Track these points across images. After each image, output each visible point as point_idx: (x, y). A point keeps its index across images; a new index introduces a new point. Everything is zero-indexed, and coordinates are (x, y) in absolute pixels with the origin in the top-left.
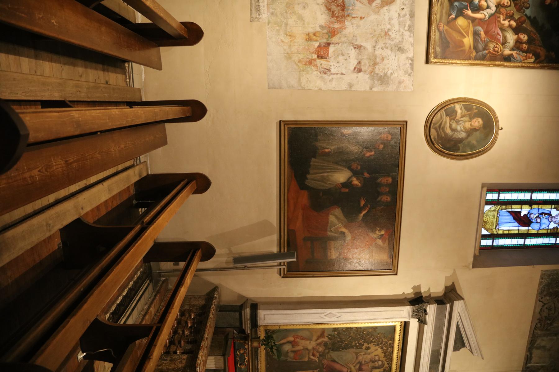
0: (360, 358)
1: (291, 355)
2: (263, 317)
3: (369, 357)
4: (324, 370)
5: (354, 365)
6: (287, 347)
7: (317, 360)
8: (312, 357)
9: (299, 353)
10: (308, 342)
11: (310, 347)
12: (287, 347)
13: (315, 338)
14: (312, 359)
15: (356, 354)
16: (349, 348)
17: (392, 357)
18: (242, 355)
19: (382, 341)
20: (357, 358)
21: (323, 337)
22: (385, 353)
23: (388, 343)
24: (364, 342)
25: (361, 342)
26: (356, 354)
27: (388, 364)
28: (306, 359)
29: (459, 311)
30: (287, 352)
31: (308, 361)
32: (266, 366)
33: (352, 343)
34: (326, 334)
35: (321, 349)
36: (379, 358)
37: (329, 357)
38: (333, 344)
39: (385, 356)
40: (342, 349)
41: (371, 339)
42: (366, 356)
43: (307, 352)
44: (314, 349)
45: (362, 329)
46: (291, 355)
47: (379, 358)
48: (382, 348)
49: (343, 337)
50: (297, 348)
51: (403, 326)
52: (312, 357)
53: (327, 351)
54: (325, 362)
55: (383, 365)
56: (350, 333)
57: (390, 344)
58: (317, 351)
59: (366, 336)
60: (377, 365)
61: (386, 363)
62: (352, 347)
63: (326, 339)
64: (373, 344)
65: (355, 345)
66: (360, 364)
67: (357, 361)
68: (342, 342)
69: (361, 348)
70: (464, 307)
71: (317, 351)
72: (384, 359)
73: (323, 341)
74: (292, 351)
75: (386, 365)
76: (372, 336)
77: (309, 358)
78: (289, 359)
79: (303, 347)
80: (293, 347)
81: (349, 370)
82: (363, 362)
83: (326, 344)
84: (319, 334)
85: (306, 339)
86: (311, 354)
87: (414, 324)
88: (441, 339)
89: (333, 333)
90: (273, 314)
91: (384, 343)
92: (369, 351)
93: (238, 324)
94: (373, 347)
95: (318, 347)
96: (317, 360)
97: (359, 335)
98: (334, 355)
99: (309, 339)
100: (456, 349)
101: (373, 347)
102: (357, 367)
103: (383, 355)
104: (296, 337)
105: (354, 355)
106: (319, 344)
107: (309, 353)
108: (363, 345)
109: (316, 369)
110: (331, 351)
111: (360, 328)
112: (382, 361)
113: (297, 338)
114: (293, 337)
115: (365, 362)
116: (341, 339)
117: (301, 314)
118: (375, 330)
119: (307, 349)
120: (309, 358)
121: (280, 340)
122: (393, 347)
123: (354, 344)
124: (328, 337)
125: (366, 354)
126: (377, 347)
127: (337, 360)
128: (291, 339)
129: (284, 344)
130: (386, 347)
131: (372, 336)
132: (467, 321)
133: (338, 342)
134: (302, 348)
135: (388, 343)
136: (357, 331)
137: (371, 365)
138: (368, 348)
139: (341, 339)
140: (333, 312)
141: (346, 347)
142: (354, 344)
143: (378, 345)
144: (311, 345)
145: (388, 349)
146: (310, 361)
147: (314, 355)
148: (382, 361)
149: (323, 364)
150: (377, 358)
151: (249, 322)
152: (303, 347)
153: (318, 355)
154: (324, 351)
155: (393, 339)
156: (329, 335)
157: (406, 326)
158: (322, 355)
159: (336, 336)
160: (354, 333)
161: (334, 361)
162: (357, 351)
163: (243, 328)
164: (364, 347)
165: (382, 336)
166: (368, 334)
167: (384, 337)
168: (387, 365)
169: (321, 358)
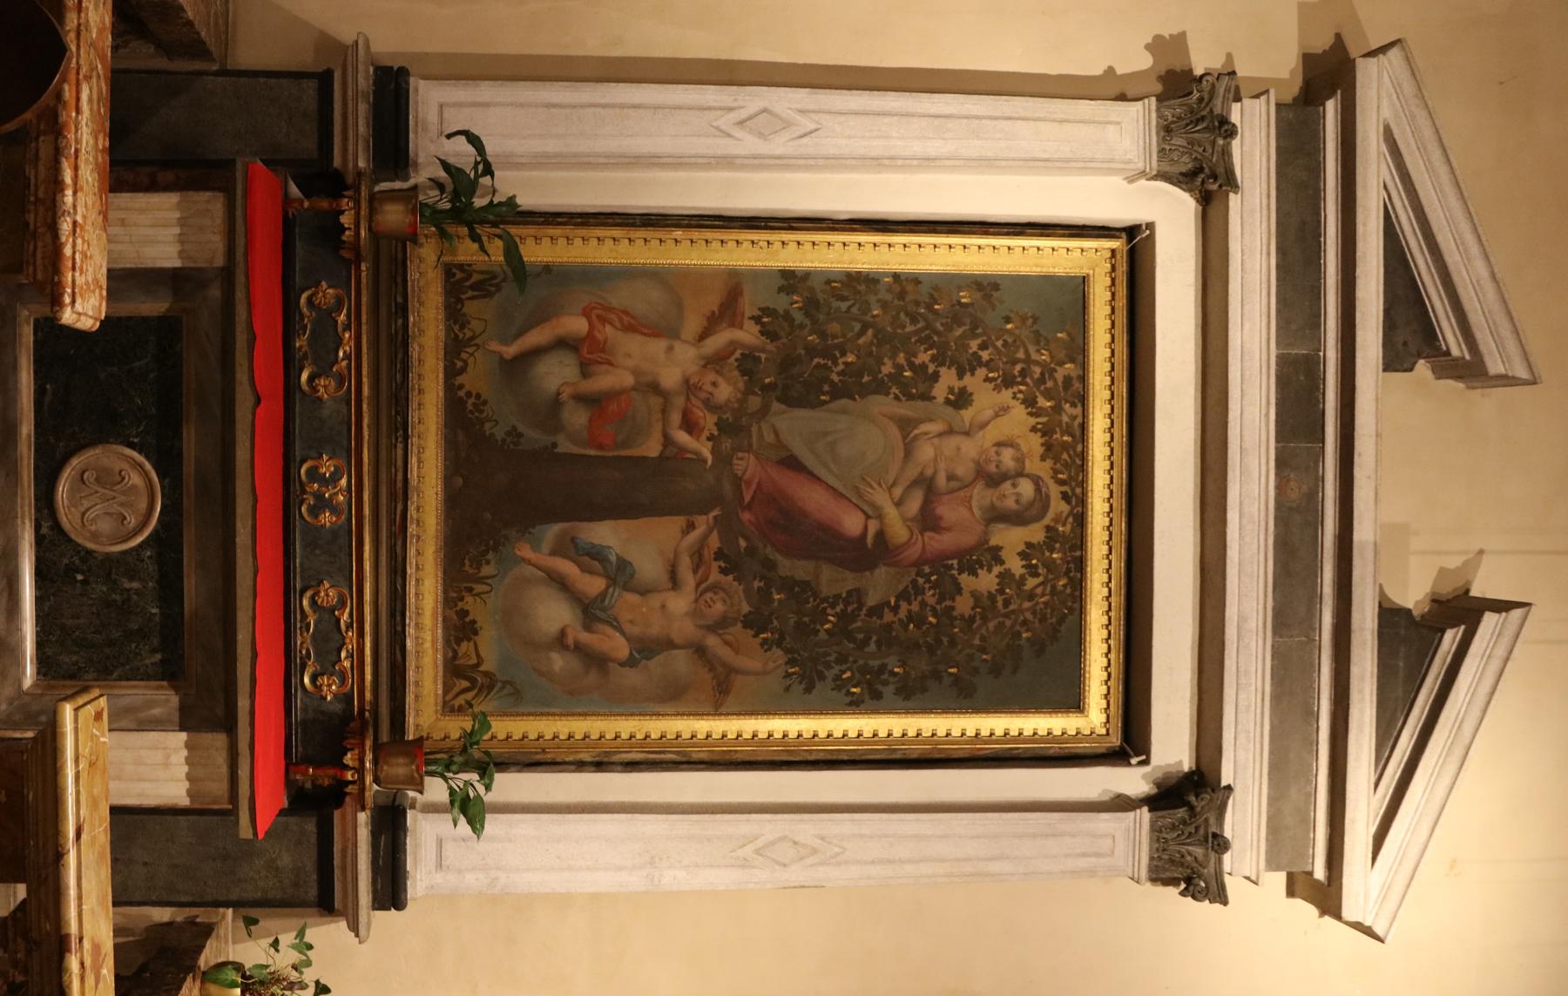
0: (926, 452)
1: (577, 418)
2: (433, 117)
3: (970, 448)
4: (746, 516)
5: (898, 492)
6: (556, 374)
7: (706, 452)
8: (682, 437)
9: (613, 407)
10: (658, 346)
11: (670, 378)
12: (556, 374)
13: (692, 325)
14: (683, 449)
15: (906, 425)
16: (865, 391)
17: (1083, 455)
18: (326, 318)
19: (1028, 360)
20: (908, 453)
21: (736, 323)
22: (1046, 432)
23: (1060, 375)
24: (939, 360)
25: (923, 357)
26: (906, 425)
27: (1065, 497)
28: (652, 448)
29: (1386, 113)
30: (556, 403)
31: (662, 457)
32: (447, 481)
33: (880, 363)
34: (748, 306)
35: (725, 392)
36: (1020, 460)
37: (769, 438)
38: (786, 364)
39: (1049, 450)
40: (838, 393)
41: (974, 345)
42: (956, 440)
43: (656, 402)
44: (689, 387)
45: (925, 288)
46: (577, 418)
47: (1020, 460)
48: (1029, 402)
49: (835, 327)
50: (605, 381)
51: (1123, 268)
52: (682, 437)
53: (755, 402)
54: (746, 465)
55: (1042, 501)
56: (866, 309)
57: (1068, 381)
58: (709, 405)
59: (949, 328)
60: (1010, 503)
61: (1054, 491)
62: (880, 387)
63: (748, 334)
64: (981, 372)
65: (896, 377)
66: (926, 484)
67: (912, 473)
68: (827, 353)
69: (927, 397)
70: (1408, 88)
71: (709, 405)
72: (1043, 469)
73: (733, 345)
74: (580, 398)
75: (1058, 506)
76: (974, 327)
77: (668, 441)
78: (565, 446)
79: (636, 372)
80: (585, 370)
81: (873, 527)
82: (941, 481)
83: (748, 363)
84: (713, 302)
85: (655, 333)
86: (676, 418)
87: (1172, 216)
88: (1315, 292)
89: (781, 303)
90: (486, 105)
91: (1037, 370)
92: (967, 414)
93: (309, 145)
94: (985, 398)
95: (711, 377)
96: (706, 452)
97: (914, 320)
98: (793, 426)
99: (664, 330)
100: (1395, 361)
101: (985, 398)
102: (914, 505)
103: (1035, 443)
104: (598, 314)
105: (894, 431)
106: (714, 362)
107: (664, 411)
108: (935, 377)
109: (704, 511)
110: (776, 406)
111: (916, 279)
112: (1037, 481)
113: (603, 320)
114: (586, 313)
115: (951, 478)
116: (823, 335)
117: (622, 106)
118: (987, 297)
119: (655, 388)
120: (668, 441)
121: (521, 333)
122: (1082, 399)
123: (887, 368)
124: (757, 320)
125: (950, 431)
126: (1007, 395)
127: (809, 460)
128: (576, 325)
129: (537, 352)
130: (1048, 395)
131: (974, 327)
132: (1431, 170)
133: (811, 351)
134: (629, 380)
135: (1060, 375)
136: (902, 295)
137: (981, 496)
138: (961, 399)
139: (823, 335)
140: (778, 108)
141: (857, 385)
142: (887, 368)
143: (1008, 382)
144: (674, 363)
145: (1057, 409)
146: (673, 457)
147: (689, 425)
148: (1037, 481)
149: (737, 481)
150: (1007, 458)
151: (363, 108)
152: (636, 372)
153: (709, 422)
154: (742, 402)
155: (1079, 352)
156: (766, 311)
157: (1136, 246)
158: (732, 428)
159: (799, 317)
160: (884, 305)
161: (792, 464)
162: (905, 409)
163: (337, 162)
164: (940, 391)
165: (1025, 333)
166: (958, 313)
167: (1037, 338)
168: (1064, 507)
169: (727, 444)
